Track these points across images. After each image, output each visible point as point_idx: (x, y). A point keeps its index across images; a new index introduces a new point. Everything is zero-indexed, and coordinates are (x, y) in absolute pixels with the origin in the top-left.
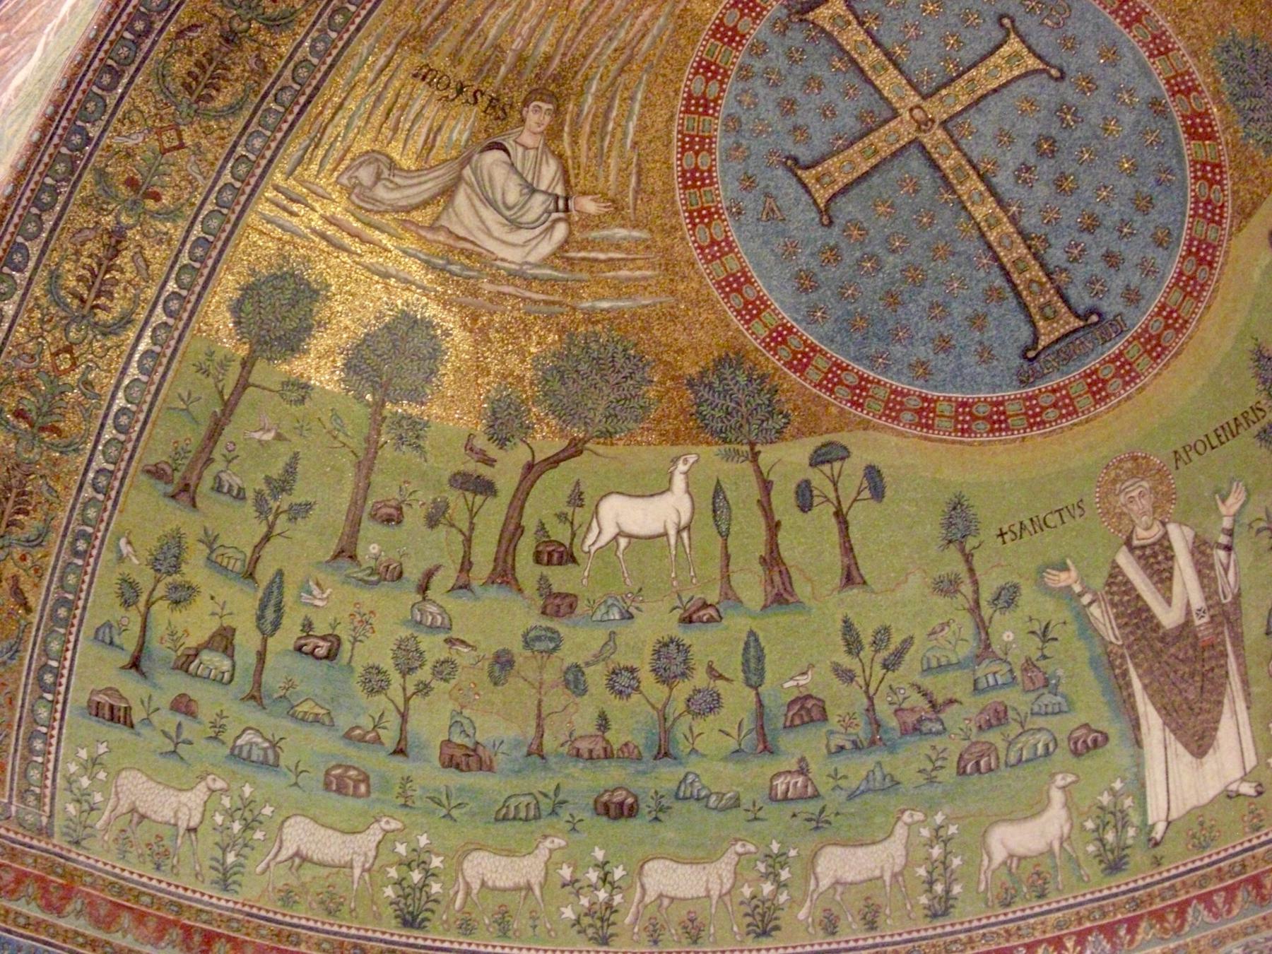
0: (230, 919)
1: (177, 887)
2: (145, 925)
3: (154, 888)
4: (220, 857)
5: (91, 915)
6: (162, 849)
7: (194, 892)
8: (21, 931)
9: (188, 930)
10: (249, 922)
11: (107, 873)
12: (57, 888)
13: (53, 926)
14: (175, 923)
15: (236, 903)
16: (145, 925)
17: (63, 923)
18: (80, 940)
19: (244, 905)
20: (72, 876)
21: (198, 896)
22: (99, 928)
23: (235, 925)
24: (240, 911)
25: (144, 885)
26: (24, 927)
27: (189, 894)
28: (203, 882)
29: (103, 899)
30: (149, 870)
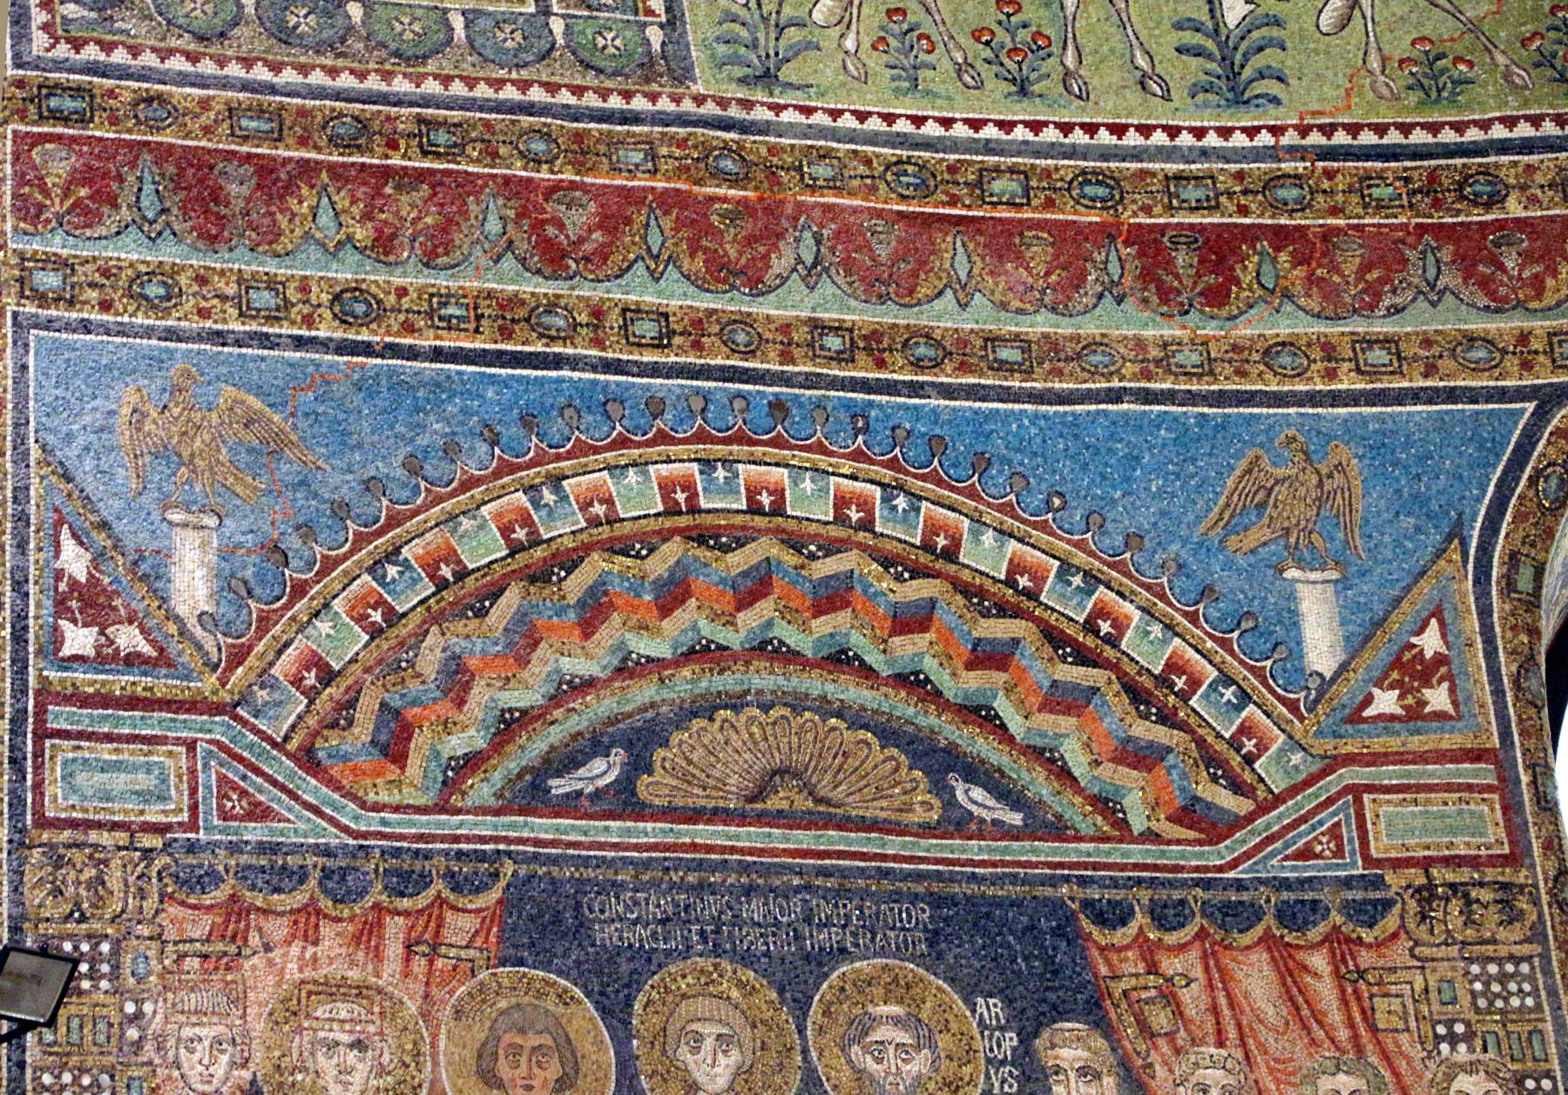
0: (1274, 181)
1: (1091, 129)
2: (1019, 258)
3: (1024, 148)
4: (1204, 16)
5: (848, 265)
6: (1023, 35)
7: (1145, 130)
8: (649, 357)
9: (1149, 243)
10: (1330, 175)
11: (873, 139)
12: (731, 217)
13: (746, 321)
14: (1107, 234)
15: (1276, 131)
16: (1019, 258)
17: (765, 308)
18: (834, 343)
19: (1304, 131)
20: (772, 174)
21: (1159, 138)
22: (882, 299)
23: (1289, 193)
24: (1295, 152)
25: (989, 147)
26: (658, 346)
27: (1132, 139)
28: (1167, 98)
29: (879, 214)
30: (995, 101)
